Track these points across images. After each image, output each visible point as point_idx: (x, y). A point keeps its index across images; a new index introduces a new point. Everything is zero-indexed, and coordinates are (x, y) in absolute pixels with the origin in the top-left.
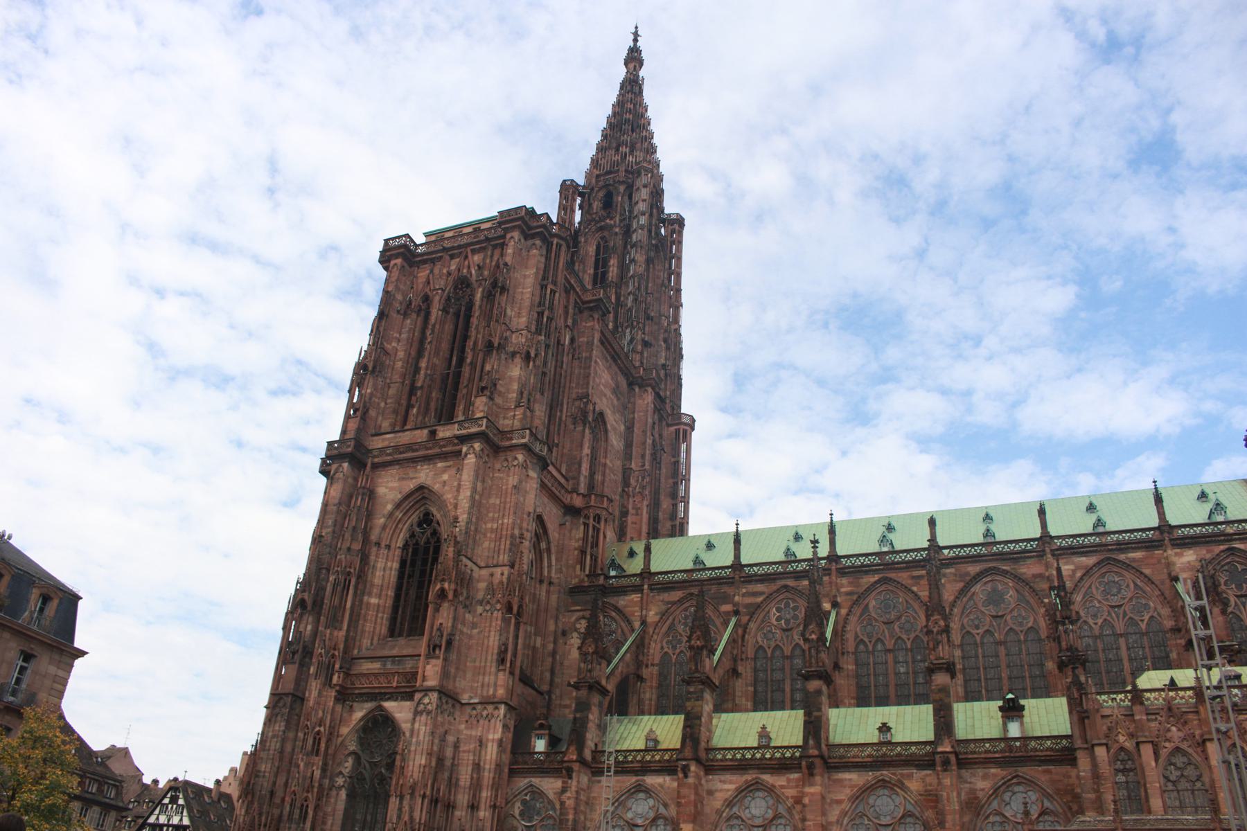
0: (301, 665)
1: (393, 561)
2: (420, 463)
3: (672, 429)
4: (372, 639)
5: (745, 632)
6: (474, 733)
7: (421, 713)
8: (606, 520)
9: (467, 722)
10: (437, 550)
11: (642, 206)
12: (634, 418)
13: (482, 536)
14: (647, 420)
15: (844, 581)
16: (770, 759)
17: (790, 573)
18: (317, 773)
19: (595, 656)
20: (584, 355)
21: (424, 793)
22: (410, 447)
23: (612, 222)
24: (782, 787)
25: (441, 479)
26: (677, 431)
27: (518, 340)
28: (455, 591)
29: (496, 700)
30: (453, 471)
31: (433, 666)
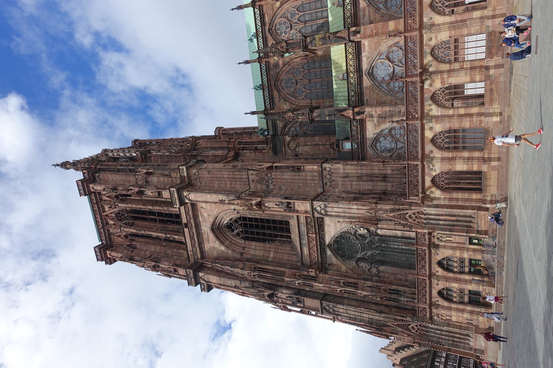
0: (305, 296)
2: (200, 231)
3: (222, 136)
4: (293, 254)
6: (340, 183)
7: (326, 211)
9: (334, 188)
10: (244, 219)
12: (209, 147)
13: (233, 189)
14: (211, 141)
18: (369, 283)
20: (166, 160)
21: (375, 203)
22: (192, 238)
25: (207, 218)
26: (223, 134)
30: (202, 210)
31: (299, 207)
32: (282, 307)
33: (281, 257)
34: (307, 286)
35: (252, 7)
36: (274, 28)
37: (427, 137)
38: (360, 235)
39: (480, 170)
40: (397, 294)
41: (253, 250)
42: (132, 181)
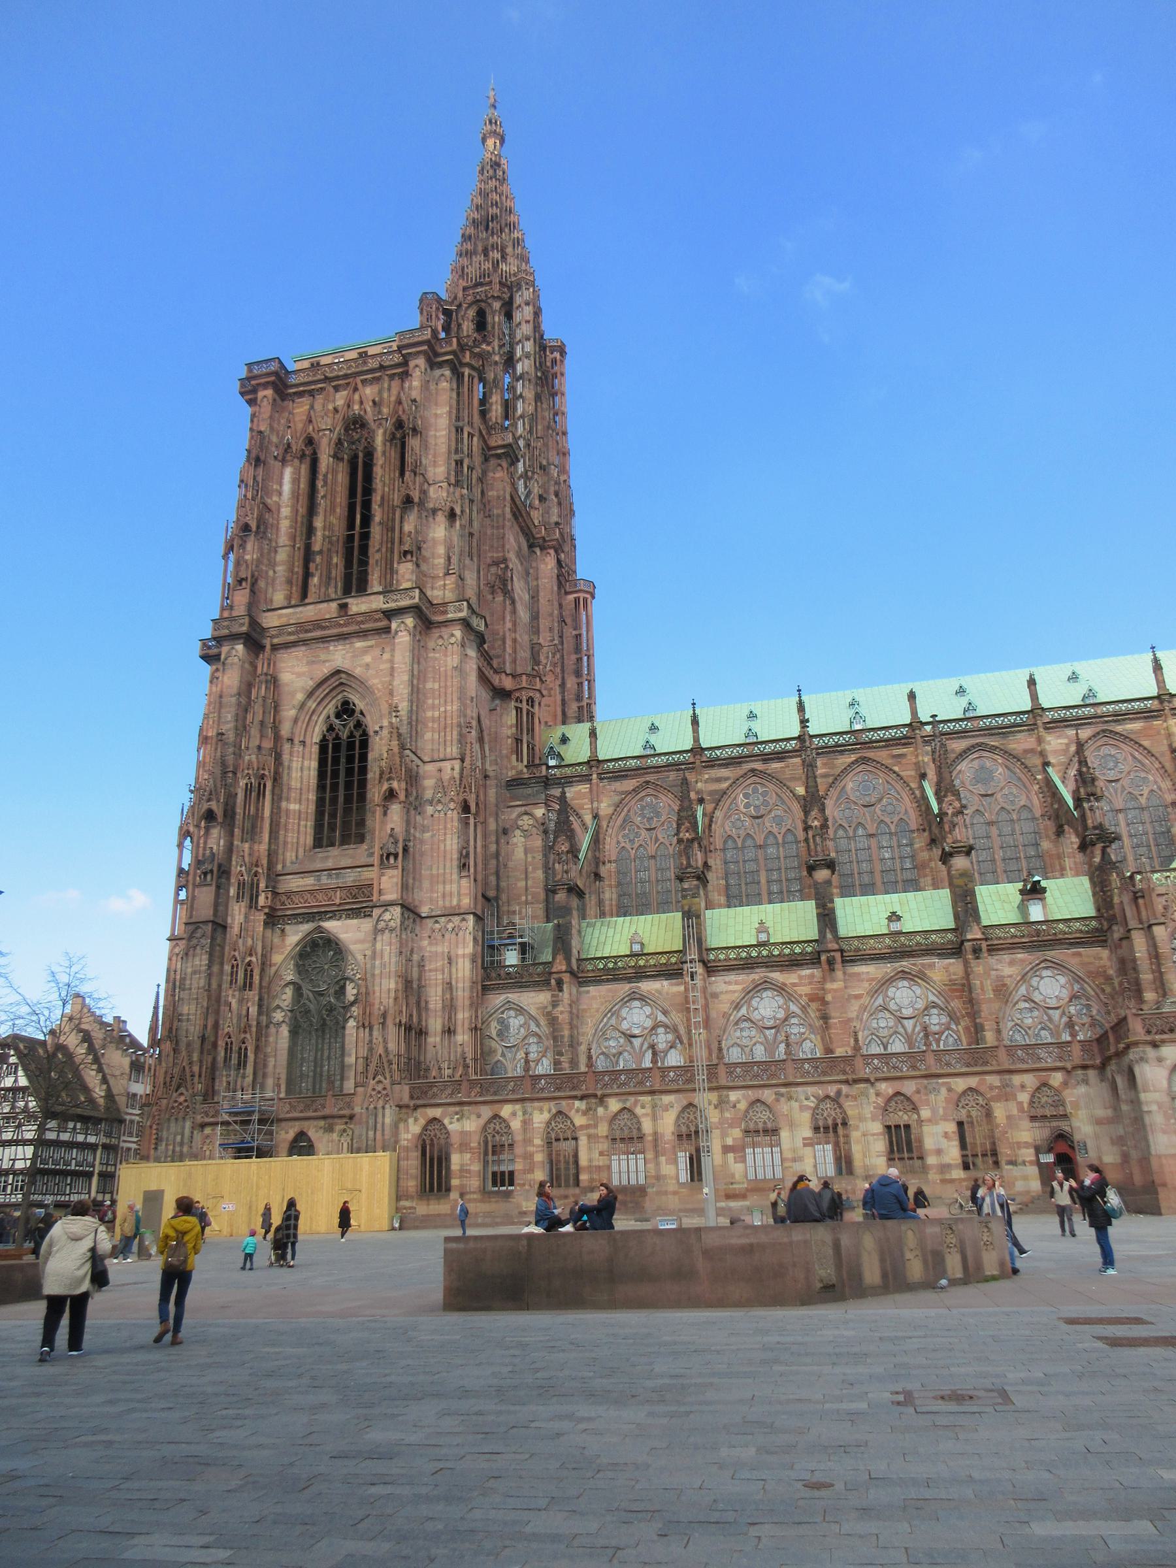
0: (218, 887)
1: (310, 759)
2: (332, 643)
3: (571, 597)
5: (711, 821)
6: (439, 949)
7: (382, 931)
8: (540, 704)
9: (430, 937)
10: (364, 744)
11: (526, 329)
12: (538, 585)
18: (253, 1010)
19: (570, 856)
20: (495, 512)
22: (317, 624)
23: (489, 348)
24: (794, 985)
26: (577, 600)
27: (438, 495)
28: (406, 790)
29: (462, 911)
30: (377, 652)
31: (390, 877)
32: (185, 828)
33: (290, 827)
34: (239, 889)
36: (759, 780)
37: (501, 1109)
38: (343, 988)
39: (452, 1189)
40: (239, 1064)
41: (299, 766)
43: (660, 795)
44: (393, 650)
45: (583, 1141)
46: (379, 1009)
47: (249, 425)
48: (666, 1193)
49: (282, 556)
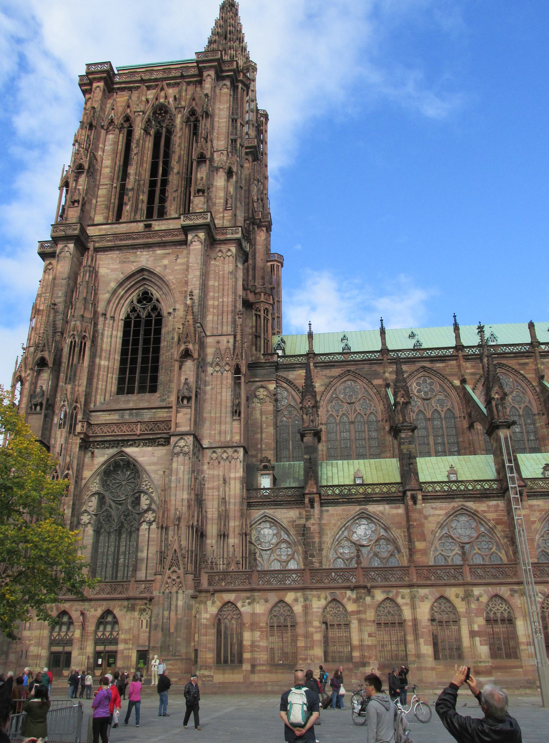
0: (46, 416)
3: (269, 264)
6: (216, 473)
7: (178, 454)
10: (159, 322)
15: (468, 365)
16: (472, 490)
17: (427, 357)
22: (128, 235)
24: (484, 512)
26: (272, 266)
29: (235, 444)
30: (173, 257)
31: (184, 414)
32: (18, 374)
33: (101, 377)
35: (456, 346)
36: (426, 374)
37: (286, 595)
41: (110, 334)
42: (219, 143)
43: (358, 381)
44: (189, 254)
45: (354, 625)
46: (175, 513)
47: (84, 106)
48: (426, 669)
49: (102, 192)
